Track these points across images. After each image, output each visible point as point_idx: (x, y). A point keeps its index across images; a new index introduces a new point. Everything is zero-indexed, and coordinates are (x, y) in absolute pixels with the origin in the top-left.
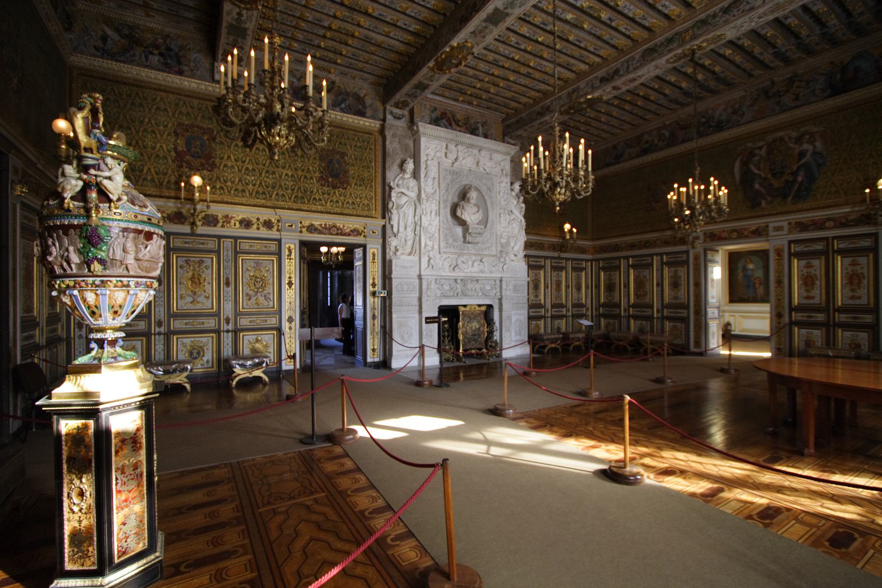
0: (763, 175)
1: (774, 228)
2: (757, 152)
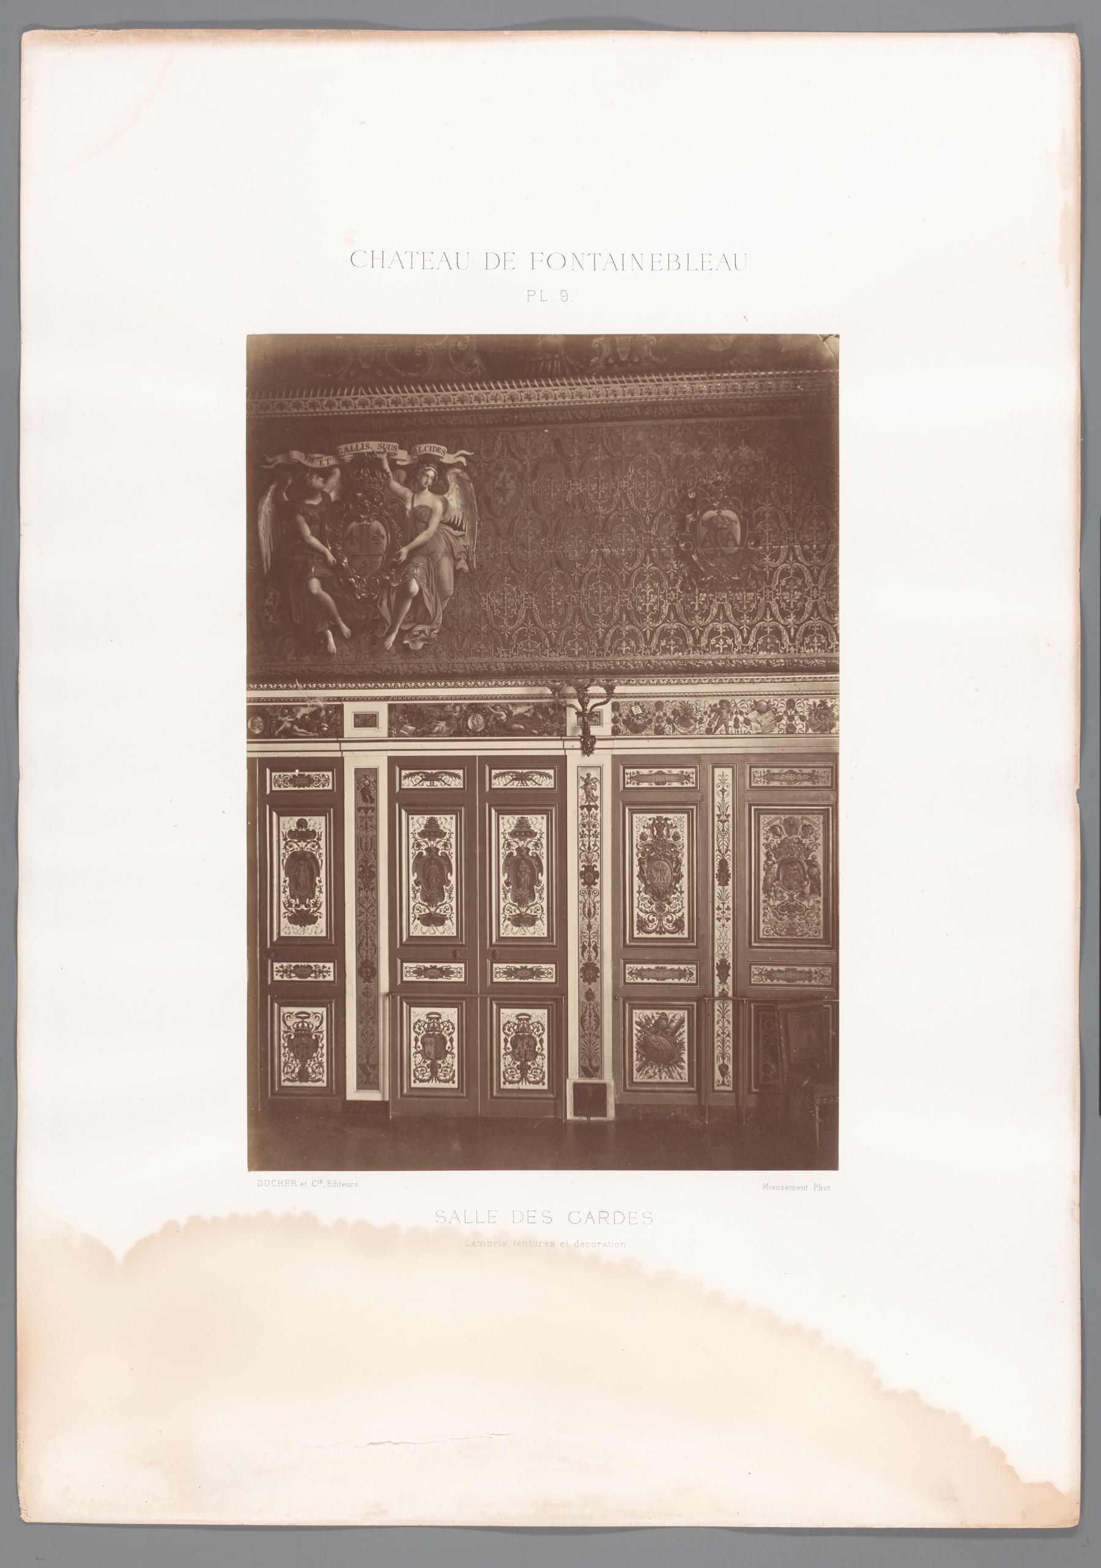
0: (331, 558)
1: (356, 716)
2: (318, 482)
